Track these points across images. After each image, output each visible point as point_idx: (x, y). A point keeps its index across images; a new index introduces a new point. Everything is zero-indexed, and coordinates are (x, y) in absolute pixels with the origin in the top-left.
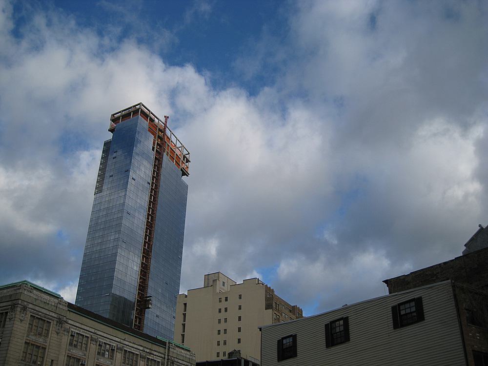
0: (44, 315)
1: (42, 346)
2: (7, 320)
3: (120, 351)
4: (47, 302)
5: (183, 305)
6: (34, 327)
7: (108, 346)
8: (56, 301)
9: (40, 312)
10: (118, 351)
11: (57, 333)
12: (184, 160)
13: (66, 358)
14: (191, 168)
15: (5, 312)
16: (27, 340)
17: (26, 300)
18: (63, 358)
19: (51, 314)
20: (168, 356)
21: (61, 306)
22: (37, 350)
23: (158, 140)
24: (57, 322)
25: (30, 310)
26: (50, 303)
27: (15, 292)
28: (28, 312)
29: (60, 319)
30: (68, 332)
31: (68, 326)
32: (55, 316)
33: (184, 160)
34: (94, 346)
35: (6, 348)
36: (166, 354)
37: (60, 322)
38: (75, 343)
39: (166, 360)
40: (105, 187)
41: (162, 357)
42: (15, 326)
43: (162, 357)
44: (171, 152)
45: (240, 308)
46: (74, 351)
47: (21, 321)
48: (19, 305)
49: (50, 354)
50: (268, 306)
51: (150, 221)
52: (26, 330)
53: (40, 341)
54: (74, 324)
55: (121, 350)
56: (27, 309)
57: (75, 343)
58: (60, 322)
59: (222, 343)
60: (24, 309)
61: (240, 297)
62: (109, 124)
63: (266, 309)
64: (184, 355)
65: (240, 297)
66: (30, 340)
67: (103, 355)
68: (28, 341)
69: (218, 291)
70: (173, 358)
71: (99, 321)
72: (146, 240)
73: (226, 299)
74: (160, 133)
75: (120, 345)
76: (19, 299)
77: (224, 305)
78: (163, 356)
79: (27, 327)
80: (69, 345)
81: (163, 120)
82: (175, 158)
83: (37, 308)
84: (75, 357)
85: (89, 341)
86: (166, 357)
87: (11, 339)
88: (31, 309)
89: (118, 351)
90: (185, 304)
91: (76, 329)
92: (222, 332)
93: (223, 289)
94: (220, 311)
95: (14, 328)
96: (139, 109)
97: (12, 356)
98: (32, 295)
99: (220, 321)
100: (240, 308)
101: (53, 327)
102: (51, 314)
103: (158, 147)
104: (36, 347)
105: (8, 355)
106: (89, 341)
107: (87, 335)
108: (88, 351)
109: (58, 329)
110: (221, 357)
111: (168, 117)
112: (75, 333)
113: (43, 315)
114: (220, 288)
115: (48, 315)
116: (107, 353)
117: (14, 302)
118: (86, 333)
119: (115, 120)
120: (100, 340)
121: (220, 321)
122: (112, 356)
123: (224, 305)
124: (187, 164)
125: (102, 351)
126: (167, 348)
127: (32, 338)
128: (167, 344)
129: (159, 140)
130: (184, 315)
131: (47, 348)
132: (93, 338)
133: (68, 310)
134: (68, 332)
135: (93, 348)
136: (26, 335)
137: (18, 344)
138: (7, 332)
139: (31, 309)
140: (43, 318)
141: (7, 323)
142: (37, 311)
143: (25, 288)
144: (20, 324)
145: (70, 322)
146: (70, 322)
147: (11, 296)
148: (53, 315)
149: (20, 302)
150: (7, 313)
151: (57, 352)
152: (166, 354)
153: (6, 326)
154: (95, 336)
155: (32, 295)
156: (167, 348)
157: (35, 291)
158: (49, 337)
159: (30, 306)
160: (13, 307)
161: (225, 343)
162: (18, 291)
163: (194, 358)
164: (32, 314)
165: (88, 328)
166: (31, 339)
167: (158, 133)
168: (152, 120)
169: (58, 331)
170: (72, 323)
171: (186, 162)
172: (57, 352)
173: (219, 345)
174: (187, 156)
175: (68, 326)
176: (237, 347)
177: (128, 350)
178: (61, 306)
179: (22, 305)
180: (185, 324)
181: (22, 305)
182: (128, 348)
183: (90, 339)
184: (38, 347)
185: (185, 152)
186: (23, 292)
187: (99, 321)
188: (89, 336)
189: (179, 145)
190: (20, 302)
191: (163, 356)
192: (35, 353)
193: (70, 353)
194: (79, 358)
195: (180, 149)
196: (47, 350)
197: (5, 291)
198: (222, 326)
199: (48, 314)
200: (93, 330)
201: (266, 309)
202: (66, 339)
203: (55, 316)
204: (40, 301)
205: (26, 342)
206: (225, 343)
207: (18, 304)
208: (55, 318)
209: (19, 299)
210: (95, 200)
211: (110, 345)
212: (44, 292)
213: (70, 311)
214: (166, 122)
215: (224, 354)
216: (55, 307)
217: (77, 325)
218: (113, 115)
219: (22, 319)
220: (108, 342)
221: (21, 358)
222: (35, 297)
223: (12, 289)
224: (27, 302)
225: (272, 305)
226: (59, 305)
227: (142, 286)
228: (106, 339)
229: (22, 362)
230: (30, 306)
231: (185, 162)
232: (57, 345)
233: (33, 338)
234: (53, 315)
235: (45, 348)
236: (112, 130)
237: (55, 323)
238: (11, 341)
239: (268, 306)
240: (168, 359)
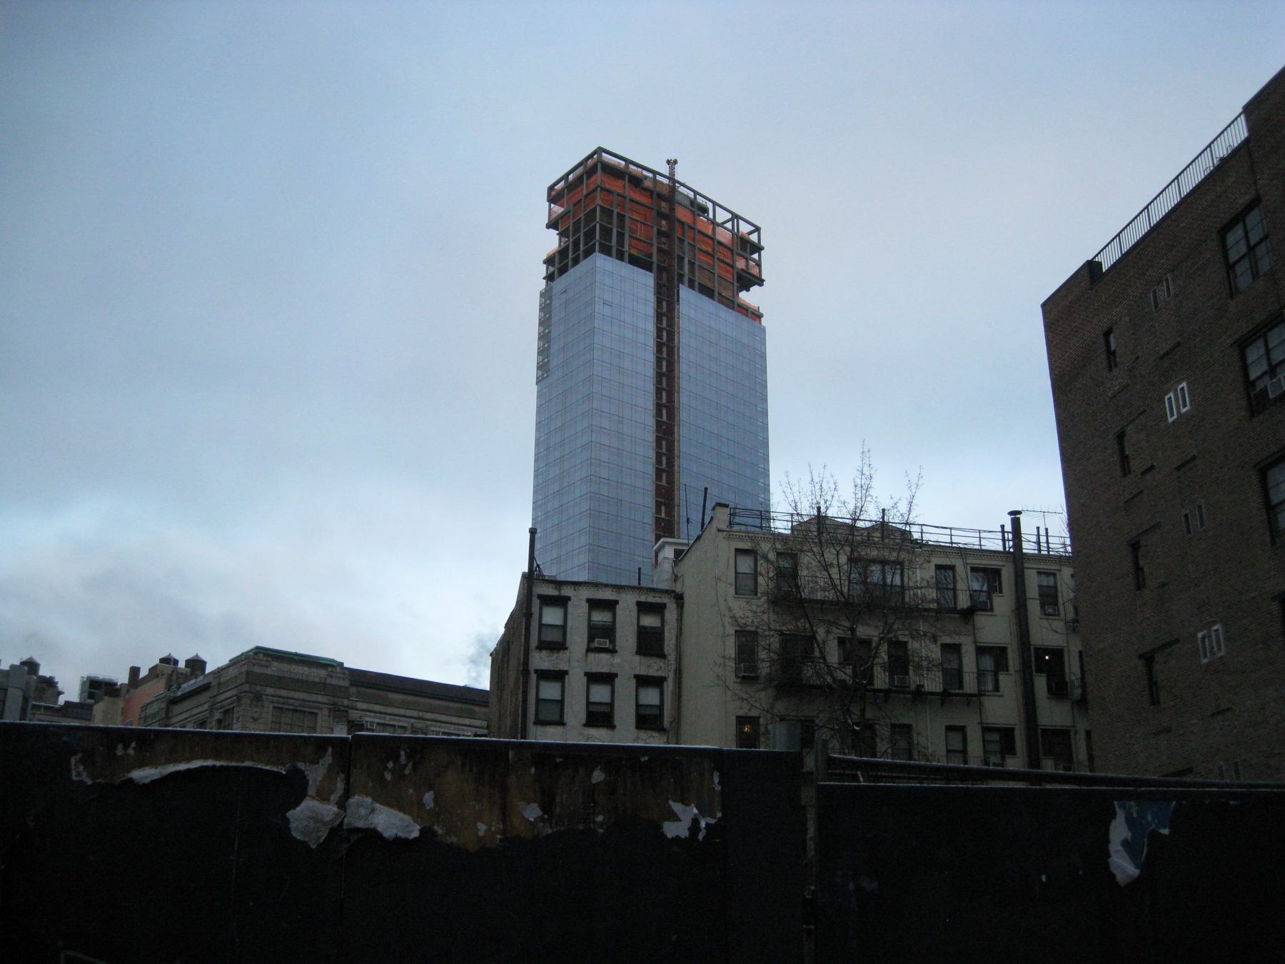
8: (323, 673)
14: (769, 263)
21: (334, 682)
24: (330, 710)
29: (335, 704)
33: (744, 249)
40: (554, 362)
47: (255, 720)
62: (541, 210)
81: (665, 170)
96: (595, 166)
98: (269, 671)
103: (663, 239)
111: (676, 162)
113: (297, 703)
119: (554, 197)
124: (756, 256)
129: (664, 222)
145: (359, 705)
148: (320, 698)
157: (275, 664)
160: (239, 699)
165: (401, 711)
168: (636, 181)
171: (753, 253)
174: (754, 238)
185: (744, 228)
189: (722, 216)
195: (729, 225)
200: (415, 714)
210: (540, 395)
218: (551, 188)
230: (270, 691)
236: (552, 225)
237: (326, 712)
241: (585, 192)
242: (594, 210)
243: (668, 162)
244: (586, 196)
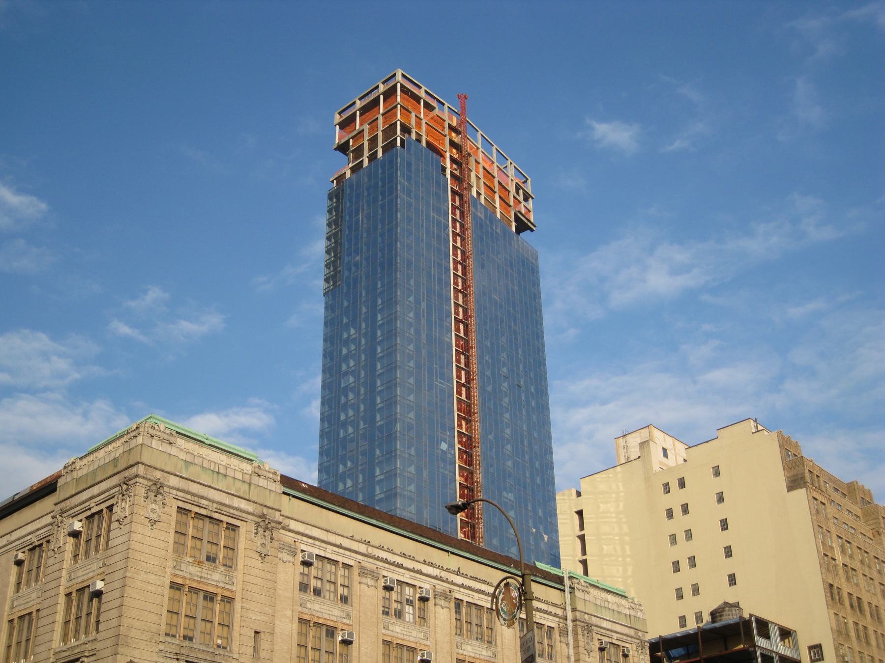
0: (215, 505)
1: (220, 592)
2: (115, 525)
3: (442, 602)
4: (222, 471)
5: (577, 517)
6: (190, 542)
7: (408, 591)
8: (247, 467)
9: (202, 497)
10: (438, 601)
11: (263, 557)
12: (518, 193)
13: (296, 625)
15: (107, 508)
16: (176, 575)
17: (158, 466)
18: (287, 628)
19: (236, 503)
20: (574, 610)
22: (210, 605)
23: (451, 151)
24: (258, 525)
25: (174, 492)
26: (230, 473)
27: (126, 448)
28: (169, 500)
29: (263, 517)
30: (294, 554)
31: (289, 538)
32: (250, 508)
33: (518, 193)
34: (370, 592)
35: (117, 603)
36: (569, 608)
37: (266, 524)
38: (314, 583)
39: (570, 624)
41: (555, 615)
42: (134, 536)
43: (555, 615)
44: (485, 176)
45: (721, 498)
46: (316, 607)
47: (153, 522)
48: (138, 479)
49: (247, 616)
50: (795, 483)
51: (462, 334)
52: (171, 549)
53: (214, 578)
54: (307, 532)
55: (446, 596)
56: (166, 489)
57: (314, 583)
58: (266, 524)
59: (688, 592)
60: (157, 488)
61: (717, 472)
63: (789, 491)
64: (615, 608)
65: (717, 472)
66: (184, 578)
67: (399, 614)
68: (180, 581)
69: (656, 467)
70: (587, 617)
71: (374, 522)
72: (460, 379)
73: (682, 484)
74: (454, 135)
75: (442, 586)
76: (138, 463)
77: (676, 498)
78: (560, 612)
79: (171, 541)
80: (301, 590)
82: (496, 189)
83: (194, 488)
84: (321, 621)
85: (356, 577)
86: (570, 616)
87: (128, 574)
88: (179, 490)
89: (438, 601)
90: (580, 513)
91: (313, 546)
92: (684, 564)
93: (666, 465)
94: (670, 514)
95: (134, 545)
97: (137, 624)
98: (173, 451)
99: (673, 539)
100: (721, 498)
101: (247, 538)
102: (236, 503)
103: (455, 166)
104: (205, 598)
105: (125, 621)
106: (356, 577)
107: (346, 561)
108: (356, 605)
109: (263, 545)
110: (692, 626)
112: (311, 555)
114: (661, 463)
115: (229, 506)
116: (408, 609)
117: (127, 474)
118: (344, 556)
120: (385, 573)
121: (673, 539)
122: (423, 618)
123: (676, 498)
125: (394, 605)
126: (567, 589)
127: (191, 572)
128: (567, 582)
129: (454, 151)
130: (582, 538)
131: (238, 599)
132: (362, 568)
133: (284, 493)
134: (294, 554)
135: (368, 595)
136: (170, 564)
137: (150, 588)
138: (117, 557)
139: (179, 490)
140: (216, 516)
141: (112, 535)
142: (194, 495)
143: (152, 431)
144: (147, 530)
146: (293, 525)
147: (116, 460)
148: (243, 505)
149: (141, 470)
150: (110, 508)
151: (270, 611)
152: (569, 608)
153: (111, 544)
154: (369, 564)
155: (173, 451)
156: (567, 589)
158: (240, 566)
159: (173, 481)
161: (696, 590)
162: (133, 443)
163: (640, 615)
164: (181, 504)
166: (187, 576)
167: (450, 134)
169: (264, 551)
170: (300, 527)
172: (270, 611)
173: (680, 596)
175: (289, 538)
176: (730, 595)
177: (466, 599)
178: (262, 482)
179: (149, 480)
180: (586, 560)
181: (149, 480)
182: (464, 594)
183: (356, 571)
184: (209, 597)
186: (148, 441)
187: (374, 522)
188: (351, 563)
190: (141, 470)
191: (560, 612)
192: (201, 607)
193: (306, 611)
194: (332, 624)
196: (238, 605)
197: (101, 454)
198: (682, 552)
199: (227, 502)
200: (362, 548)
201: (790, 489)
202: (289, 573)
203: (250, 508)
204: (198, 469)
205: (174, 586)
206: (696, 590)
207: (137, 476)
208: (248, 513)
209: (138, 463)
211: (414, 586)
212: (210, 445)
213: (289, 495)
214: (463, 108)
215: (699, 617)
216: (246, 486)
217: (316, 533)
219: (154, 517)
220: (406, 577)
221: (163, 627)
222: (182, 456)
223: (118, 443)
224: (163, 471)
225: (803, 478)
226: (255, 479)
227: (467, 487)
228: (402, 570)
229: (169, 639)
230: (173, 481)
231: (521, 198)
232: (266, 593)
233: (194, 570)
234: (243, 505)
235: (228, 600)
237: (253, 528)
238: (128, 581)
239: (795, 483)
240: (575, 620)
241: (381, 111)
242: (396, 122)
243: (459, 97)
244: (383, 115)
